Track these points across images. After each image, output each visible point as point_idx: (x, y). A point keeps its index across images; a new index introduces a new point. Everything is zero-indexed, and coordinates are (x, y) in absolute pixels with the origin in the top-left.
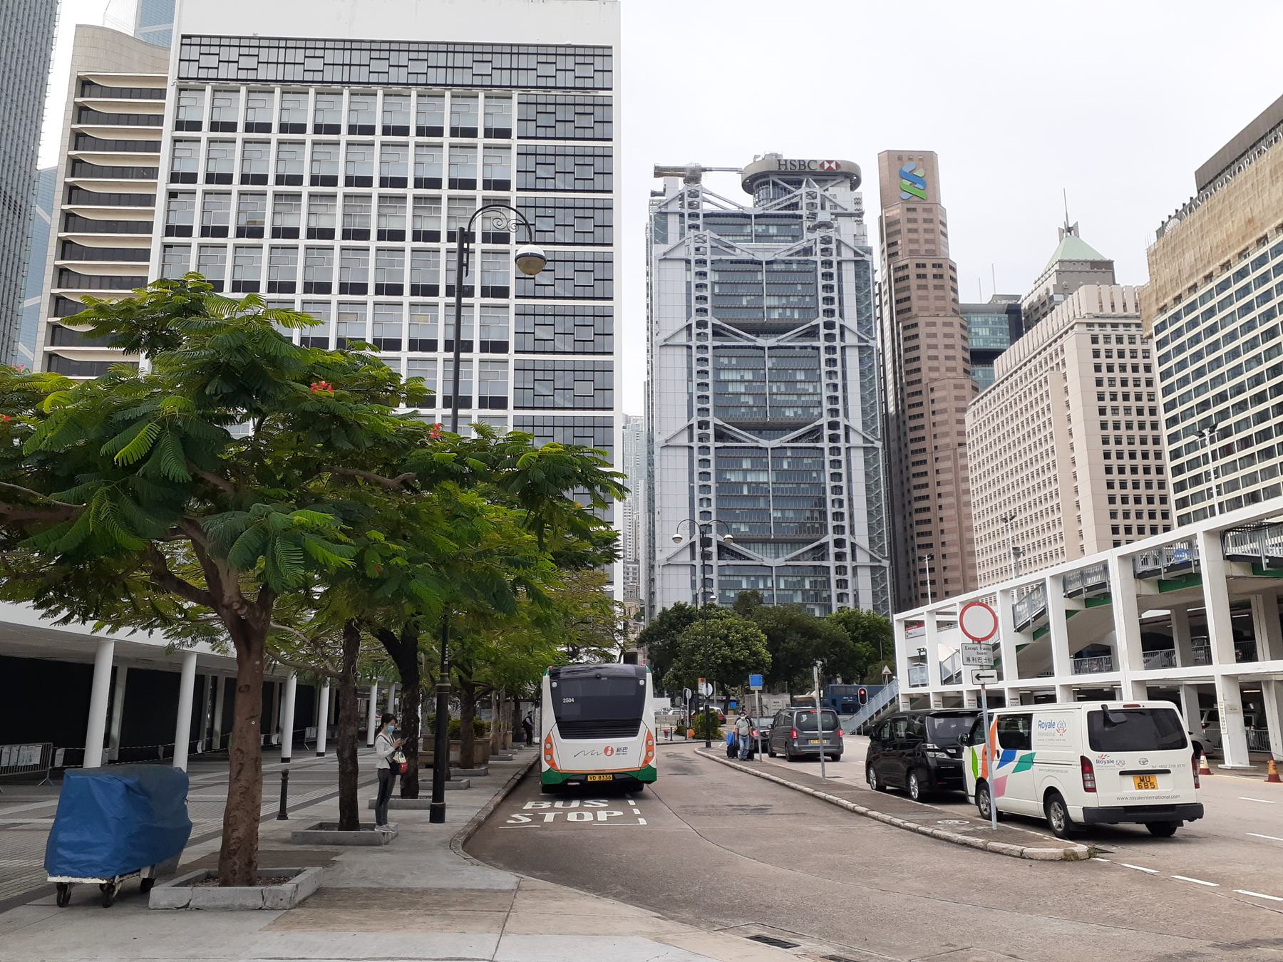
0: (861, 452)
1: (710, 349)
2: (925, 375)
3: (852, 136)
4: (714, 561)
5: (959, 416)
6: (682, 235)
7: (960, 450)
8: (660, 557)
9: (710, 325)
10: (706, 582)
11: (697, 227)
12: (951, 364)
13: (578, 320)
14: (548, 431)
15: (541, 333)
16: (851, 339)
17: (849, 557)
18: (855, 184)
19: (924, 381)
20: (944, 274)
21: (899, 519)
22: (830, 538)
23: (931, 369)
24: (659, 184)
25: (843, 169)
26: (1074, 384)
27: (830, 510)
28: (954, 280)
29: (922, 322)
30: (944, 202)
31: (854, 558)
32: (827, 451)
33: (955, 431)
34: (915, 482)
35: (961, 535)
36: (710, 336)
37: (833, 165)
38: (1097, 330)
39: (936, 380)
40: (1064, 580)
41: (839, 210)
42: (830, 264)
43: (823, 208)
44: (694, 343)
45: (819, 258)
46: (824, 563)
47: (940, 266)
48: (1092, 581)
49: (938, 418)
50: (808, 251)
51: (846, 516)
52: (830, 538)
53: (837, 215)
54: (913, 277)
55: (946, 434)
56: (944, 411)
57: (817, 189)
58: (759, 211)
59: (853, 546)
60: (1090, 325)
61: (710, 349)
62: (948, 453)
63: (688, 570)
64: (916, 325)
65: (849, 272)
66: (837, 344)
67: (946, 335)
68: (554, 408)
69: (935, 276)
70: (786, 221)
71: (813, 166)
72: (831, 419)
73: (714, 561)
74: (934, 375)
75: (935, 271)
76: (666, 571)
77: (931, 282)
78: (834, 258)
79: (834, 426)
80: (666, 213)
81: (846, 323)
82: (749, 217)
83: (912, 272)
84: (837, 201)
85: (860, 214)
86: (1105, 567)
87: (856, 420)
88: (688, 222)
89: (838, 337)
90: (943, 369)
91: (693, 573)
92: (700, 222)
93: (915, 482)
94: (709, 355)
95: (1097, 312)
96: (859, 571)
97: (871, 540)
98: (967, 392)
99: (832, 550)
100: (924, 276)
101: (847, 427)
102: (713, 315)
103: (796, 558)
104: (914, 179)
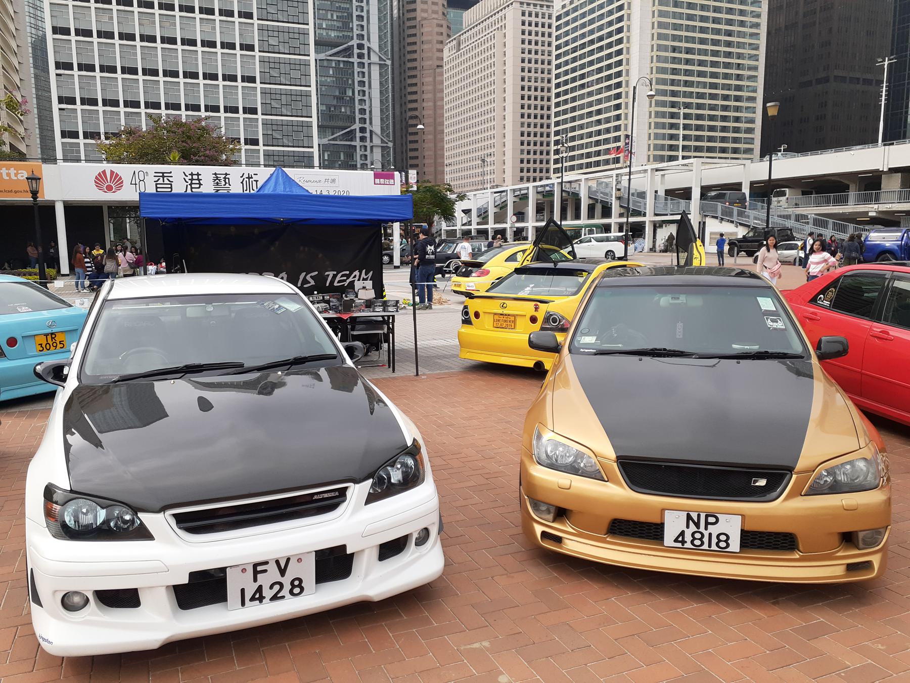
0: (377, 67)
2: (419, 14)
5: (439, 46)
7: (438, 70)
12: (435, 8)
13: (291, 35)
14: (278, 97)
15: (273, 41)
17: (368, 140)
19: (418, 19)
22: (357, 126)
23: (423, 11)
26: (509, 41)
27: (358, 107)
31: (371, 141)
32: (356, 65)
33: (435, 57)
35: (435, 128)
38: (525, 7)
39: (425, 19)
40: (514, 191)
46: (353, 143)
48: (523, 192)
49: (425, 47)
51: (367, 112)
55: (430, 59)
56: (429, 42)
59: (371, 132)
60: (522, 3)
68: (280, 84)
72: (358, 42)
79: (360, 46)
86: (528, 188)
87: (375, 44)
90: (430, 11)
97: (382, 129)
98: (444, 30)
99: (358, 135)
101: (369, 48)
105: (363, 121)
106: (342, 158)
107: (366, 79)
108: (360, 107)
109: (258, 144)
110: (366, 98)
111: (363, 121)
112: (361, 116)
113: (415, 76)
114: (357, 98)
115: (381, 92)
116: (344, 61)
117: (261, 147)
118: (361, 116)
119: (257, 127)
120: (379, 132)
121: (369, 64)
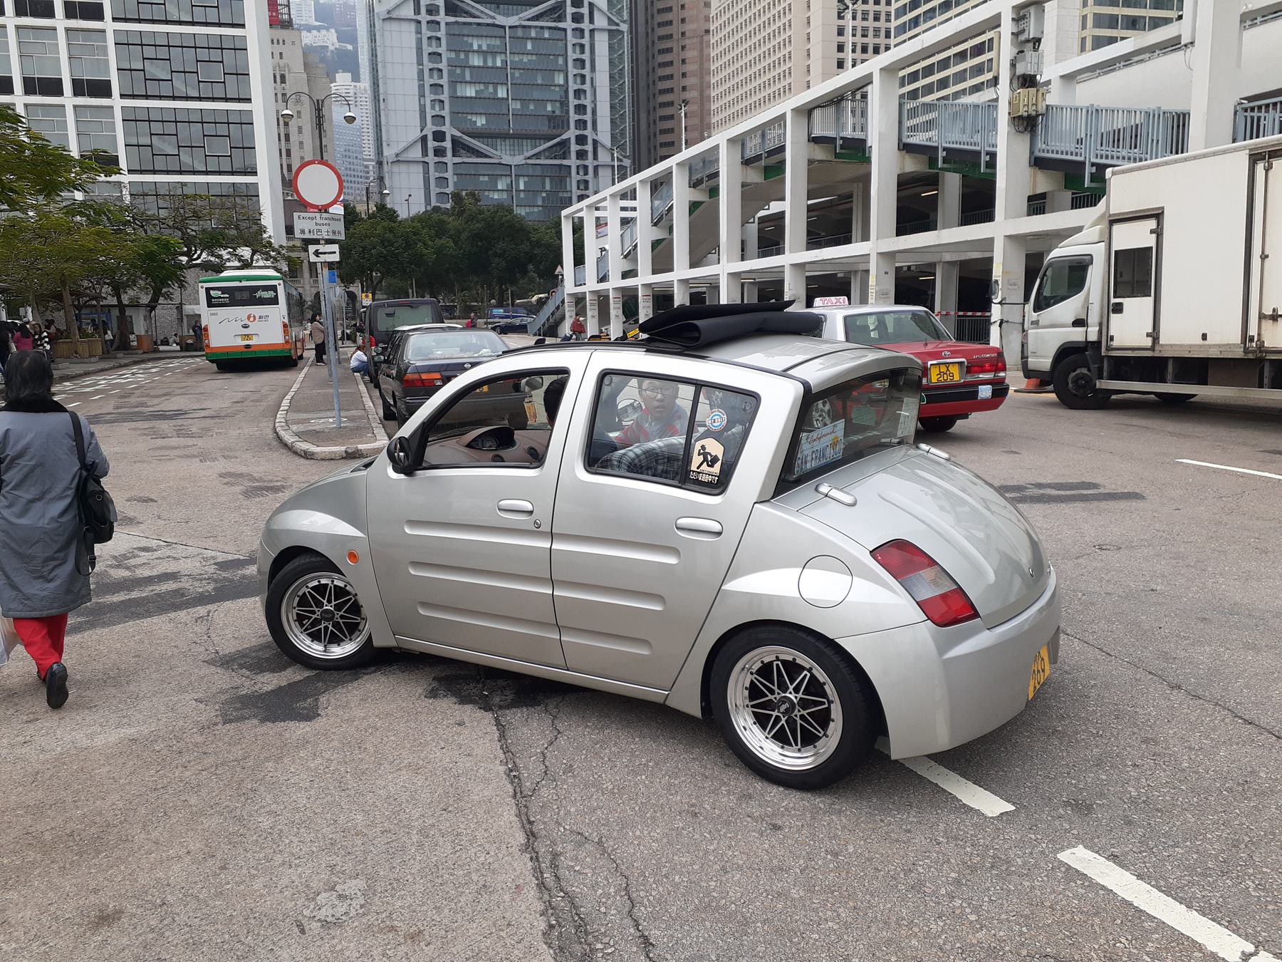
4: (449, 158)
8: (388, 152)
10: (442, 181)
17: (590, 155)
21: (643, 115)
22: (571, 134)
27: (573, 102)
32: (569, 32)
34: (661, 72)
46: (565, 162)
51: (589, 110)
52: (571, 134)
59: (595, 142)
62: (695, 40)
63: (420, 168)
73: (449, 158)
76: (396, 168)
91: (426, 172)
93: (661, 72)
96: (601, 171)
97: (613, 137)
99: (574, 147)
103: (537, 156)
105: (581, 124)
106: (548, 187)
107: (586, 56)
108: (577, 102)
109: (108, 94)
110: (587, 87)
111: (581, 124)
112: (578, 117)
113: (670, 50)
114: (573, 86)
115: (611, 77)
116: (550, 28)
117: (117, 102)
118: (578, 117)
119: (104, 50)
120: (608, 144)
121: (592, 31)
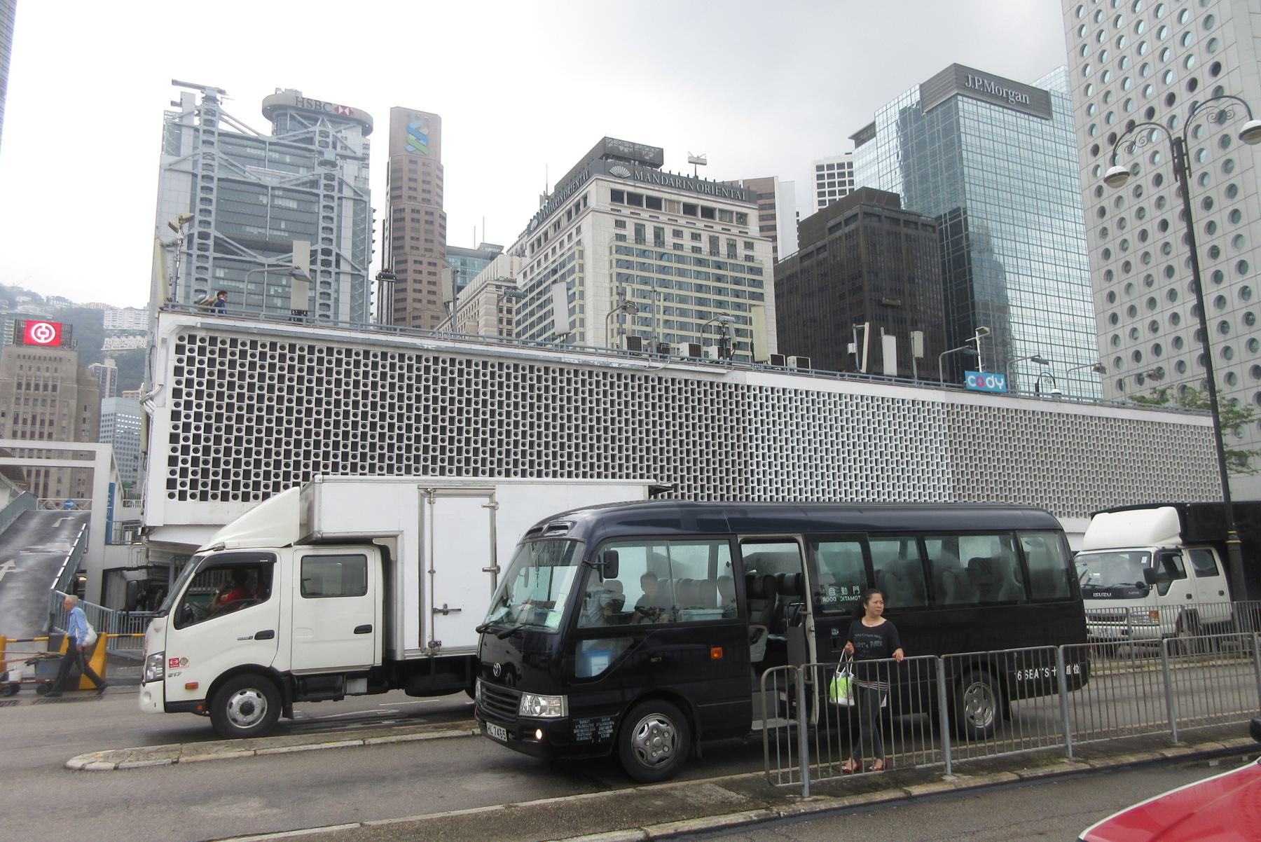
1: (211, 259)
2: (410, 304)
3: (368, 87)
6: (195, 148)
9: (212, 237)
11: (212, 143)
16: (345, 267)
18: (367, 129)
20: (436, 221)
24: (176, 93)
25: (356, 116)
28: (444, 228)
29: (411, 259)
30: (445, 160)
36: (212, 248)
37: (347, 111)
41: (348, 153)
42: (332, 198)
43: (335, 147)
44: (195, 252)
45: (321, 191)
47: (432, 214)
50: (314, 184)
53: (344, 157)
54: (408, 219)
57: (330, 128)
58: (274, 140)
60: (498, 287)
61: (211, 259)
64: (406, 261)
65: (348, 209)
66: (333, 269)
67: (430, 273)
69: (427, 222)
70: (299, 152)
71: (328, 108)
74: (417, 305)
75: (427, 218)
77: (423, 226)
78: (336, 194)
80: (180, 126)
81: (343, 253)
82: (264, 143)
83: (408, 215)
84: (349, 143)
85: (363, 160)
88: (203, 137)
89: (334, 264)
90: (424, 301)
92: (215, 139)
94: (209, 264)
95: (507, 275)
100: (418, 221)
102: (216, 228)
104: (419, 136)
